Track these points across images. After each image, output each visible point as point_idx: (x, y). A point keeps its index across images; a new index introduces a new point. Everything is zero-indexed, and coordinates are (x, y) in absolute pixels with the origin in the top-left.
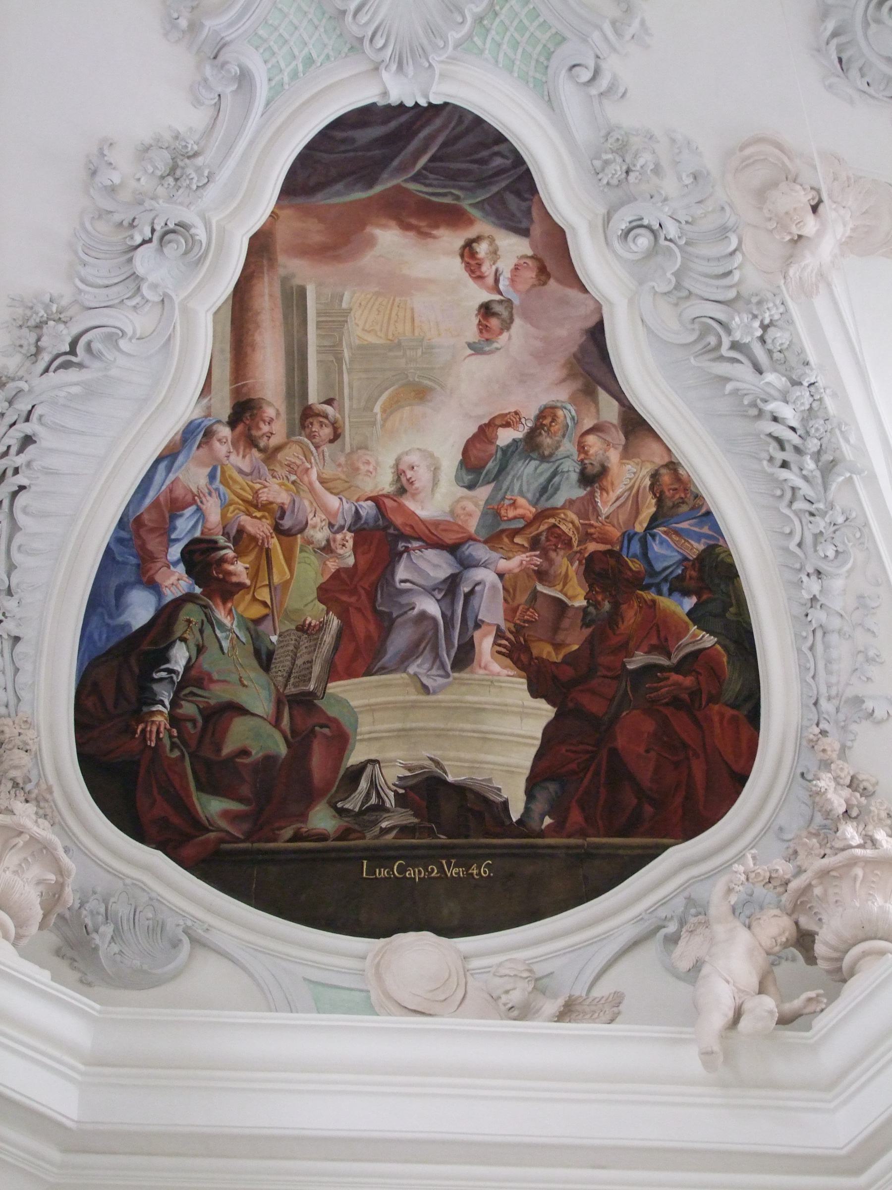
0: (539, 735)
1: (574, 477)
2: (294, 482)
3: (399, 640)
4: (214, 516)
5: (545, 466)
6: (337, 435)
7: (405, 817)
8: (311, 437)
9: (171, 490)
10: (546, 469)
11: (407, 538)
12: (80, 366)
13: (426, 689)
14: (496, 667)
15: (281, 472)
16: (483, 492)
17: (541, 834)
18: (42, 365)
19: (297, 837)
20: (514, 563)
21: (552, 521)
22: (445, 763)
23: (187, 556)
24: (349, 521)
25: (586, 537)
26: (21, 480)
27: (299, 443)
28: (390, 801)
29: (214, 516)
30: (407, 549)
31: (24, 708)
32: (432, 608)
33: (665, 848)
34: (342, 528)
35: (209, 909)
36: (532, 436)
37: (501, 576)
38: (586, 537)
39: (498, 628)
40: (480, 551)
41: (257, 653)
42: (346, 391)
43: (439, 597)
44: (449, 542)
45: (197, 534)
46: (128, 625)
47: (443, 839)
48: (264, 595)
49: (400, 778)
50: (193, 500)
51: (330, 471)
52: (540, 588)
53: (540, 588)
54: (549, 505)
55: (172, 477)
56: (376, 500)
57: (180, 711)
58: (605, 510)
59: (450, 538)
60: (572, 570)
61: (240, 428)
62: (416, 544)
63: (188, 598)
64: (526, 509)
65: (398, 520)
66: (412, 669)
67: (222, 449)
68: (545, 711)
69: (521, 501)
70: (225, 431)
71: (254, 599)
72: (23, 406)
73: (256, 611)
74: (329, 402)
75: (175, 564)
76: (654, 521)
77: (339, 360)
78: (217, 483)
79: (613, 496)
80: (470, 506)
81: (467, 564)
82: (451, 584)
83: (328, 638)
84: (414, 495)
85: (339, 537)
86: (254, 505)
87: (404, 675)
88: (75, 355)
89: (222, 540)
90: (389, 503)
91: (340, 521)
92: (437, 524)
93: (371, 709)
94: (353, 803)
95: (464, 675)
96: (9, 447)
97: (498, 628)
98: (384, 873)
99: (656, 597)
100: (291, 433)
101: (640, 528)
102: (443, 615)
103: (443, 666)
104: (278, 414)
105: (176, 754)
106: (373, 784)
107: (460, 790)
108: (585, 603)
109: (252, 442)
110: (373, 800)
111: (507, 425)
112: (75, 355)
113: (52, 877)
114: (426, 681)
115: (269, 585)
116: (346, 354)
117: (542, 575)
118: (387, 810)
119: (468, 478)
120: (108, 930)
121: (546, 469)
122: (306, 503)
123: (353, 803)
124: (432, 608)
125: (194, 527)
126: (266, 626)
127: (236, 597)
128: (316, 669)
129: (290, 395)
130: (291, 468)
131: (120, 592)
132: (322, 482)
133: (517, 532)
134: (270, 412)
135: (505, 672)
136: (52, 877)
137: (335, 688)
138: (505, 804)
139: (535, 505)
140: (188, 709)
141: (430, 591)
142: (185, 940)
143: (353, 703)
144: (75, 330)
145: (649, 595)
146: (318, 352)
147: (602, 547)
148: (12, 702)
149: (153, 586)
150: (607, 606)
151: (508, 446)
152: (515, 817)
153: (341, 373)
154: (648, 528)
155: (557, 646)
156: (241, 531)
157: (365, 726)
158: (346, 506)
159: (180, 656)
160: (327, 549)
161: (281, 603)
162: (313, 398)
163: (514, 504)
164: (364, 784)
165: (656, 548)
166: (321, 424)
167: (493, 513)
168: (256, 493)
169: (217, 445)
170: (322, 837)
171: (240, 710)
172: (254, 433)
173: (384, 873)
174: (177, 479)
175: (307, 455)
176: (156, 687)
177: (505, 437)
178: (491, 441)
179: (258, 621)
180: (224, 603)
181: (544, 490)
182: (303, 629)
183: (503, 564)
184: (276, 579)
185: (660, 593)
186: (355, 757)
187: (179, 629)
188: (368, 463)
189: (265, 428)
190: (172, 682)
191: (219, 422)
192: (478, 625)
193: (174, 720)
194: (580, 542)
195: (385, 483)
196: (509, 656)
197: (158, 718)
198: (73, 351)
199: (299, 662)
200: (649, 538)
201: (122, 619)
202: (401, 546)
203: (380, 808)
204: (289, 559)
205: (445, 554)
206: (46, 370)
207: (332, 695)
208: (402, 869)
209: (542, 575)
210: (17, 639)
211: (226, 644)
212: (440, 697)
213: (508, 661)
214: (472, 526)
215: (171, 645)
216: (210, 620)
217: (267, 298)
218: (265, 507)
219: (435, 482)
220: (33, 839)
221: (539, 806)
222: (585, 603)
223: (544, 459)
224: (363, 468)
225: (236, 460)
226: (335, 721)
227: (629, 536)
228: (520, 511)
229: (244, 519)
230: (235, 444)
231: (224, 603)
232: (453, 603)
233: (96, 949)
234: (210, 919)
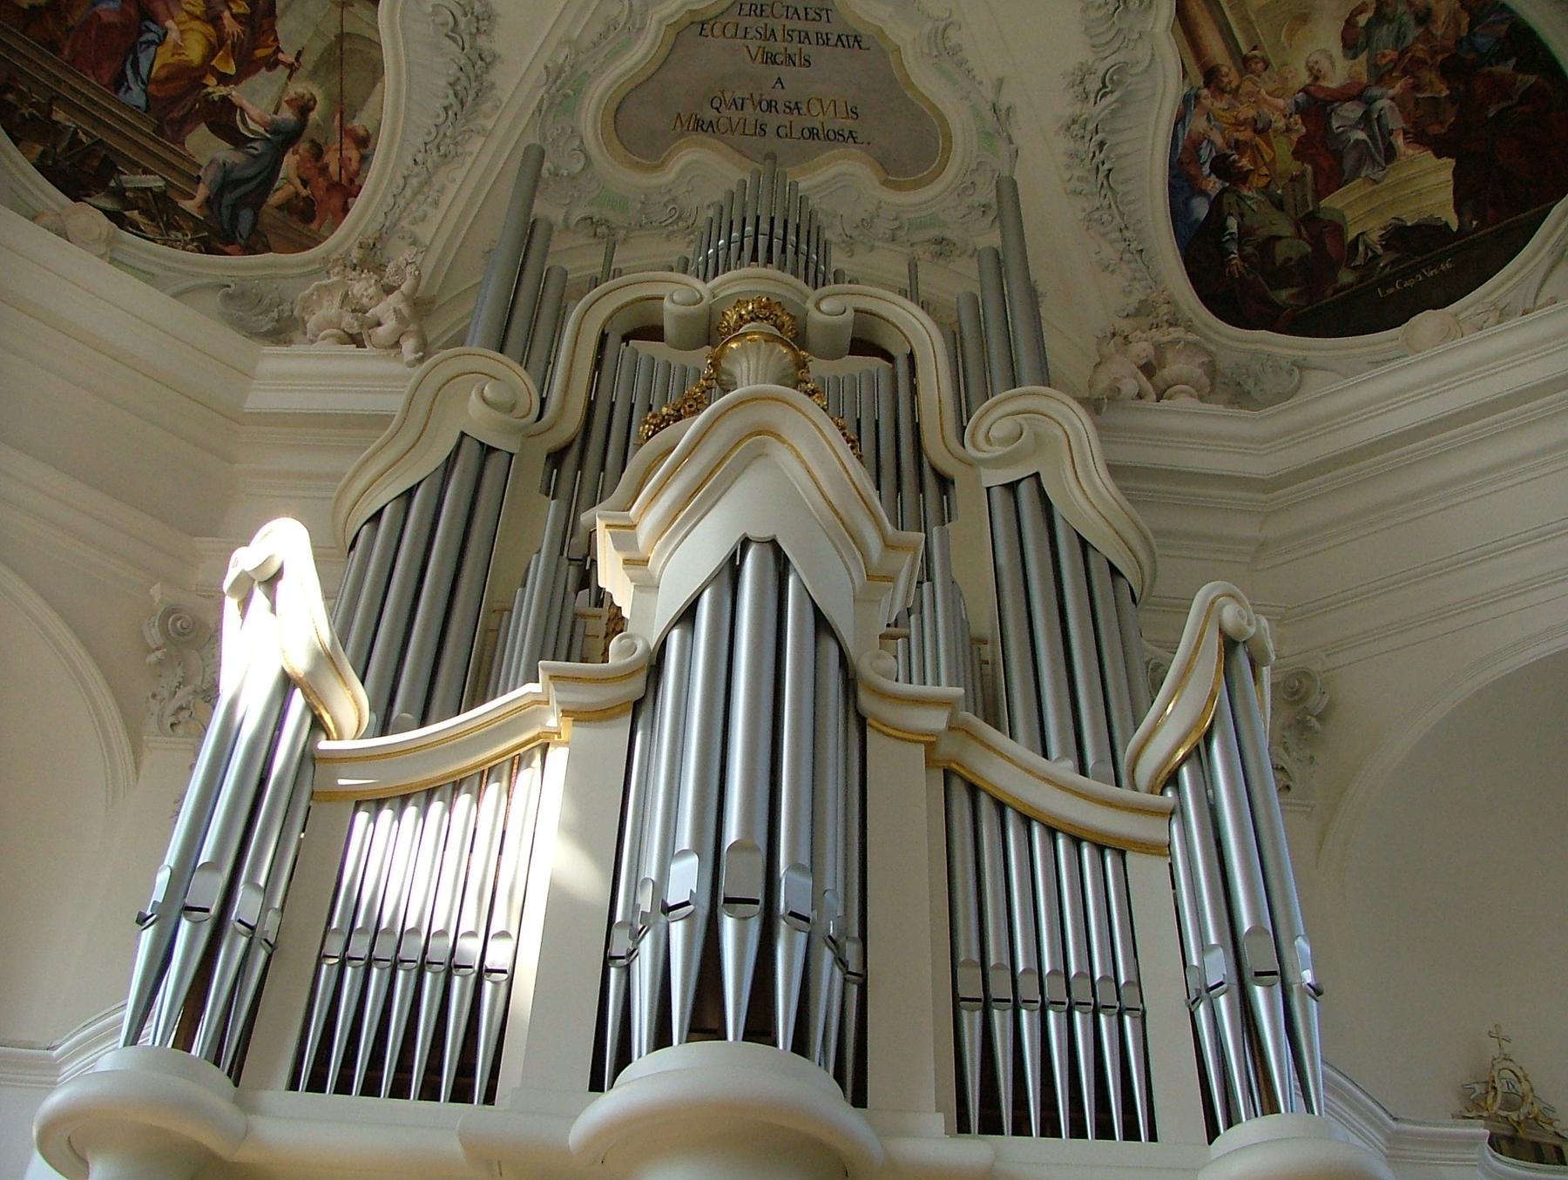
0: (1451, 178)
1: (1412, 23)
2: (1254, 102)
3: (1349, 162)
4: (1219, 140)
5: (1393, 25)
6: (1267, 65)
7: (1392, 256)
8: (1253, 72)
9: (1189, 136)
10: (1394, 26)
11: (1332, 102)
12: (1112, 92)
13: (1375, 182)
14: (1410, 152)
15: (1244, 99)
16: (1363, 57)
17: (1476, 230)
18: (1092, 101)
19: (1336, 292)
20: (1398, 88)
21: (1409, 54)
22: (1403, 217)
23: (1213, 169)
24: (1294, 110)
25: (1434, 53)
26: (1107, 166)
27: (1250, 79)
28: (1380, 251)
29: (1219, 141)
30: (1332, 110)
32: (1360, 135)
33: (1552, 207)
34: (1291, 115)
36: (1378, 12)
37: (1393, 99)
38: (1434, 53)
39: (1403, 130)
40: (1375, 91)
41: (1273, 203)
42: (1261, 38)
43: (1362, 126)
44: (1355, 94)
45: (1214, 154)
46: (1196, 220)
47: (1419, 259)
48: (1264, 171)
49: (1381, 236)
50: (1204, 137)
51: (1272, 86)
52: (1420, 95)
53: (1420, 95)
54: (1405, 45)
55: (1187, 129)
56: (1304, 90)
57: (1245, 253)
58: (1439, 33)
59: (1355, 92)
60: (1433, 76)
61: (1212, 85)
62: (1337, 104)
63: (1223, 191)
64: (1391, 54)
65: (1321, 96)
66: (1363, 174)
67: (1207, 103)
68: (1450, 163)
69: (1387, 52)
70: (1205, 92)
71: (1260, 175)
72: (1091, 127)
73: (1265, 181)
74: (1255, 48)
75: (1209, 175)
76: (1471, 25)
77: (1251, 23)
78: (1213, 123)
79: (1440, 23)
80: (1358, 68)
81: (1370, 102)
82: (1366, 116)
83: (1309, 177)
84: (1324, 77)
85: (1292, 120)
86: (1238, 124)
87: (1360, 180)
88: (1106, 87)
89: (1229, 152)
90: (1312, 88)
91: (1288, 112)
92: (1344, 87)
93: (1349, 205)
94: (1359, 261)
95: (1394, 164)
96: (1094, 153)
97: (1403, 130)
98: (1391, 290)
99: (1489, 68)
100: (1241, 76)
101: (1464, 33)
102: (1368, 136)
103: (1379, 164)
104: (1230, 70)
105: (1251, 276)
106: (1367, 247)
107: (1417, 226)
108: (1448, 92)
109: (1222, 91)
110: (1370, 254)
111: (1361, 13)
112: (1106, 87)
114: (1373, 177)
115: (1265, 164)
116: (1253, 17)
117: (1417, 87)
118: (1380, 256)
119: (1350, 54)
120: (1251, 382)
121: (1394, 26)
122: (1266, 110)
123: (1359, 261)
124: (1360, 135)
125: (1211, 150)
126: (1273, 186)
127: (1250, 178)
128: (1309, 198)
129: (1232, 55)
130: (1249, 94)
131: (1186, 204)
132: (1270, 94)
133: (1391, 71)
134: (1225, 70)
135: (1417, 151)
137: (1324, 203)
138: (1446, 224)
139: (1396, 50)
140: (1249, 250)
141: (1354, 127)
142: (1295, 368)
143: (1338, 207)
144: (1101, 73)
145: (1486, 69)
146: (1238, 23)
147: (1446, 55)
149: (1203, 193)
150: (1462, 88)
151: (1367, 24)
152: (1455, 229)
153: (1254, 28)
154: (1469, 32)
155: (1442, 123)
156: (1237, 141)
157: (1349, 217)
158: (1289, 101)
159: (1233, 224)
160: (1288, 130)
161: (1275, 171)
162: (1245, 51)
163: (1384, 56)
164: (1361, 248)
165: (1480, 40)
166: (1257, 63)
167: (1373, 66)
168: (1236, 118)
169: (1203, 101)
170: (1351, 285)
171: (1279, 238)
172: (1222, 85)
173: (1391, 290)
174: (1190, 130)
175: (1255, 83)
176: (1226, 246)
177: (1362, 20)
178: (1355, 25)
179: (1267, 186)
180: (1244, 184)
181: (1398, 38)
182: (1293, 179)
183: (1391, 92)
184: (1267, 159)
185: (1491, 65)
186: (1351, 235)
187: (1226, 209)
188: (1290, 72)
189: (1226, 80)
190: (1234, 239)
191: (1199, 88)
192: (1391, 133)
193: (1243, 258)
194: (1432, 59)
195: (1304, 78)
196: (1416, 142)
197: (1234, 262)
198: (1104, 86)
199: (1298, 198)
200: (1472, 38)
201: (1195, 216)
202: (1329, 108)
203: (1376, 256)
204: (1269, 144)
205: (1356, 102)
206: (1095, 103)
207: (1325, 207)
208: (1401, 284)
209: (1417, 87)
210: (1142, 250)
211: (1254, 207)
212: (1386, 181)
213: (1417, 146)
214: (1364, 79)
215: (1226, 219)
216: (1241, 198)
217: (1196, 8)
218: (1244, 123)
219: (1332, 63)
221: (1466, 218)
222: (1448, 92)
223: (1390, 21)
224: (1289, 76)
225: (1218, 104)
226: (1329, 221)
227: (1459, 41)
228: (1388, 58)
229: (1236, 135)
230: (1213, 96)
231: (1244, 184)
232: (1371, 128)
233: (1249, 393)
234: (1306, 353)
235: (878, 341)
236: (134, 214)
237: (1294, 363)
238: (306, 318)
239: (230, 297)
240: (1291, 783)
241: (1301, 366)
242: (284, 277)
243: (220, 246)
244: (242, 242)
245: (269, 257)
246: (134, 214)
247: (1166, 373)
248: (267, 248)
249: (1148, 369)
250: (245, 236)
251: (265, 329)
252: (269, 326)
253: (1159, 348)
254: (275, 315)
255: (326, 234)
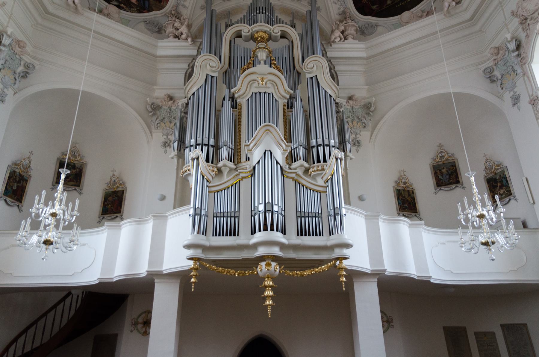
31: (347, 6)
35: (378, 21)
113: (355, 28)
120: (366, 29)
136: (355, 28)
142: (375, 26)
148: (345, 6)
220: (351, 25)
233: (365, 32)
234: (378, 22)
235: (286, 37)
236: (122, 5)
237: (375, 25)
238: (165, 30)
239: (147, 23)
240: (365, 126)
241: (377, 25)
242: (158, 17)
243: (142, 11)
244: (147, 9)
245: (153, 13)
246: (122, 5)
247: (346, 33)
248: (153, 10)
249: (343, 32)
250: (147, 8)
251: (156, 31)
252: (157, 30)
253: (345, 27)
254: (157, 27)
255: (165, 5)
